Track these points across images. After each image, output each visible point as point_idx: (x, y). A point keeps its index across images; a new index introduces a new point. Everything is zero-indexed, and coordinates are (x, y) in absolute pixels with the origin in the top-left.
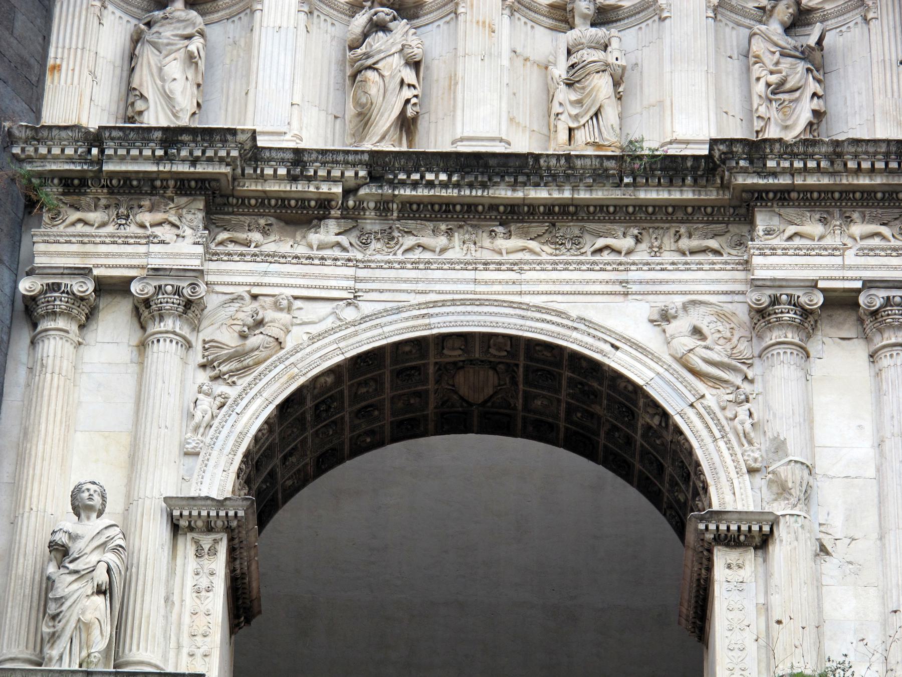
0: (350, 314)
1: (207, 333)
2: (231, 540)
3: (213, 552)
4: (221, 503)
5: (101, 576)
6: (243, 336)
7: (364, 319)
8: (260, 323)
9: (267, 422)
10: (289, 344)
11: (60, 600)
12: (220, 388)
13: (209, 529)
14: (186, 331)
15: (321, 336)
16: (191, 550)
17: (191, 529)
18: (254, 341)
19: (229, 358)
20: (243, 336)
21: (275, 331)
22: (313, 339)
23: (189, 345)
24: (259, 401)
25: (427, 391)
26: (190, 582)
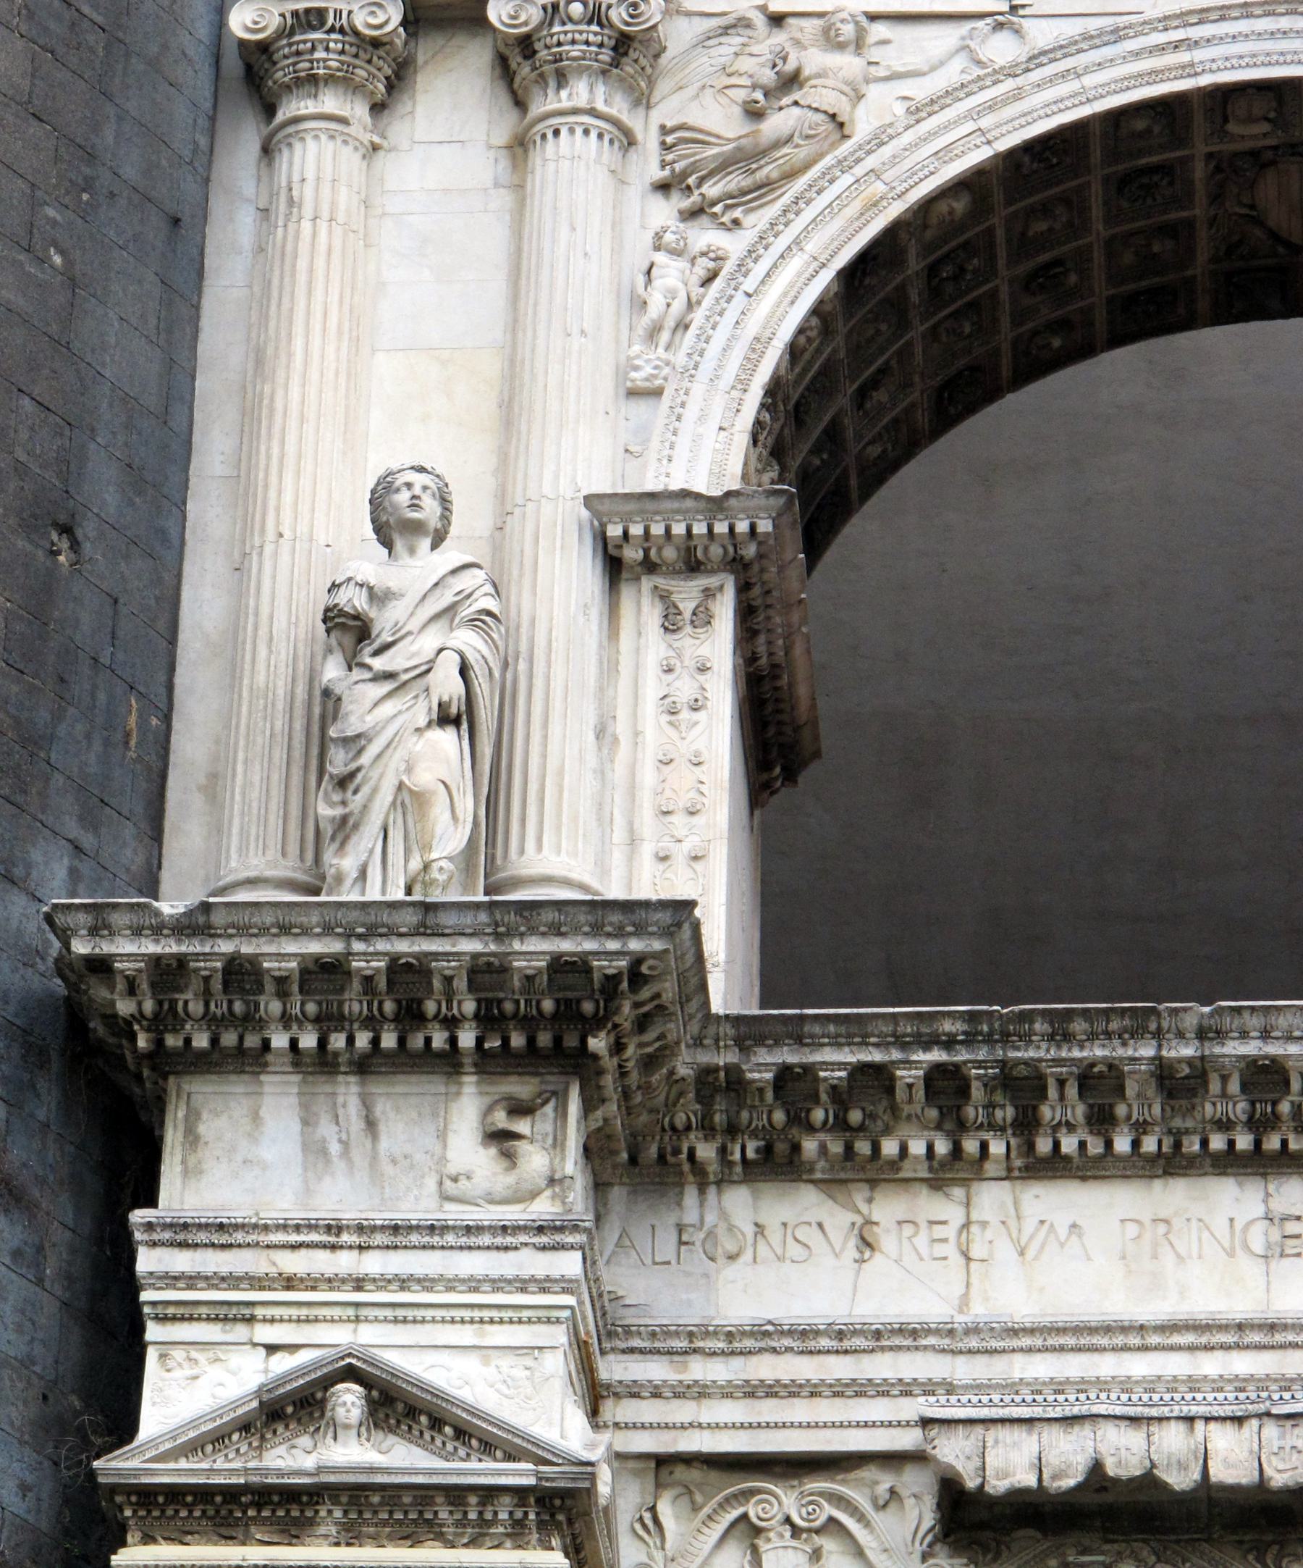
0: (1002, 49)
1: (668, 110)
2: (743, 588)
3: (702, 618)
4: (717, 505)
5: (447, 685)
6: (754, 113)
7: (1036, 59)
8: (791, 81)
9: (817, 310)
10: (863, 123)
11: (355, 743)
12: (705, 236)
13: (692, 565)
14: (619, 107)
15: (935, 104)
16: (652, 615)
17: (650, 566)
18: (779, 122)
19: (724, 166)
20: (754, 113)
21: (827, 98)
22: (918, 112)
23: (628, 140)
24: (796, 264)
25: (1190, 224)
26: (652, 688)
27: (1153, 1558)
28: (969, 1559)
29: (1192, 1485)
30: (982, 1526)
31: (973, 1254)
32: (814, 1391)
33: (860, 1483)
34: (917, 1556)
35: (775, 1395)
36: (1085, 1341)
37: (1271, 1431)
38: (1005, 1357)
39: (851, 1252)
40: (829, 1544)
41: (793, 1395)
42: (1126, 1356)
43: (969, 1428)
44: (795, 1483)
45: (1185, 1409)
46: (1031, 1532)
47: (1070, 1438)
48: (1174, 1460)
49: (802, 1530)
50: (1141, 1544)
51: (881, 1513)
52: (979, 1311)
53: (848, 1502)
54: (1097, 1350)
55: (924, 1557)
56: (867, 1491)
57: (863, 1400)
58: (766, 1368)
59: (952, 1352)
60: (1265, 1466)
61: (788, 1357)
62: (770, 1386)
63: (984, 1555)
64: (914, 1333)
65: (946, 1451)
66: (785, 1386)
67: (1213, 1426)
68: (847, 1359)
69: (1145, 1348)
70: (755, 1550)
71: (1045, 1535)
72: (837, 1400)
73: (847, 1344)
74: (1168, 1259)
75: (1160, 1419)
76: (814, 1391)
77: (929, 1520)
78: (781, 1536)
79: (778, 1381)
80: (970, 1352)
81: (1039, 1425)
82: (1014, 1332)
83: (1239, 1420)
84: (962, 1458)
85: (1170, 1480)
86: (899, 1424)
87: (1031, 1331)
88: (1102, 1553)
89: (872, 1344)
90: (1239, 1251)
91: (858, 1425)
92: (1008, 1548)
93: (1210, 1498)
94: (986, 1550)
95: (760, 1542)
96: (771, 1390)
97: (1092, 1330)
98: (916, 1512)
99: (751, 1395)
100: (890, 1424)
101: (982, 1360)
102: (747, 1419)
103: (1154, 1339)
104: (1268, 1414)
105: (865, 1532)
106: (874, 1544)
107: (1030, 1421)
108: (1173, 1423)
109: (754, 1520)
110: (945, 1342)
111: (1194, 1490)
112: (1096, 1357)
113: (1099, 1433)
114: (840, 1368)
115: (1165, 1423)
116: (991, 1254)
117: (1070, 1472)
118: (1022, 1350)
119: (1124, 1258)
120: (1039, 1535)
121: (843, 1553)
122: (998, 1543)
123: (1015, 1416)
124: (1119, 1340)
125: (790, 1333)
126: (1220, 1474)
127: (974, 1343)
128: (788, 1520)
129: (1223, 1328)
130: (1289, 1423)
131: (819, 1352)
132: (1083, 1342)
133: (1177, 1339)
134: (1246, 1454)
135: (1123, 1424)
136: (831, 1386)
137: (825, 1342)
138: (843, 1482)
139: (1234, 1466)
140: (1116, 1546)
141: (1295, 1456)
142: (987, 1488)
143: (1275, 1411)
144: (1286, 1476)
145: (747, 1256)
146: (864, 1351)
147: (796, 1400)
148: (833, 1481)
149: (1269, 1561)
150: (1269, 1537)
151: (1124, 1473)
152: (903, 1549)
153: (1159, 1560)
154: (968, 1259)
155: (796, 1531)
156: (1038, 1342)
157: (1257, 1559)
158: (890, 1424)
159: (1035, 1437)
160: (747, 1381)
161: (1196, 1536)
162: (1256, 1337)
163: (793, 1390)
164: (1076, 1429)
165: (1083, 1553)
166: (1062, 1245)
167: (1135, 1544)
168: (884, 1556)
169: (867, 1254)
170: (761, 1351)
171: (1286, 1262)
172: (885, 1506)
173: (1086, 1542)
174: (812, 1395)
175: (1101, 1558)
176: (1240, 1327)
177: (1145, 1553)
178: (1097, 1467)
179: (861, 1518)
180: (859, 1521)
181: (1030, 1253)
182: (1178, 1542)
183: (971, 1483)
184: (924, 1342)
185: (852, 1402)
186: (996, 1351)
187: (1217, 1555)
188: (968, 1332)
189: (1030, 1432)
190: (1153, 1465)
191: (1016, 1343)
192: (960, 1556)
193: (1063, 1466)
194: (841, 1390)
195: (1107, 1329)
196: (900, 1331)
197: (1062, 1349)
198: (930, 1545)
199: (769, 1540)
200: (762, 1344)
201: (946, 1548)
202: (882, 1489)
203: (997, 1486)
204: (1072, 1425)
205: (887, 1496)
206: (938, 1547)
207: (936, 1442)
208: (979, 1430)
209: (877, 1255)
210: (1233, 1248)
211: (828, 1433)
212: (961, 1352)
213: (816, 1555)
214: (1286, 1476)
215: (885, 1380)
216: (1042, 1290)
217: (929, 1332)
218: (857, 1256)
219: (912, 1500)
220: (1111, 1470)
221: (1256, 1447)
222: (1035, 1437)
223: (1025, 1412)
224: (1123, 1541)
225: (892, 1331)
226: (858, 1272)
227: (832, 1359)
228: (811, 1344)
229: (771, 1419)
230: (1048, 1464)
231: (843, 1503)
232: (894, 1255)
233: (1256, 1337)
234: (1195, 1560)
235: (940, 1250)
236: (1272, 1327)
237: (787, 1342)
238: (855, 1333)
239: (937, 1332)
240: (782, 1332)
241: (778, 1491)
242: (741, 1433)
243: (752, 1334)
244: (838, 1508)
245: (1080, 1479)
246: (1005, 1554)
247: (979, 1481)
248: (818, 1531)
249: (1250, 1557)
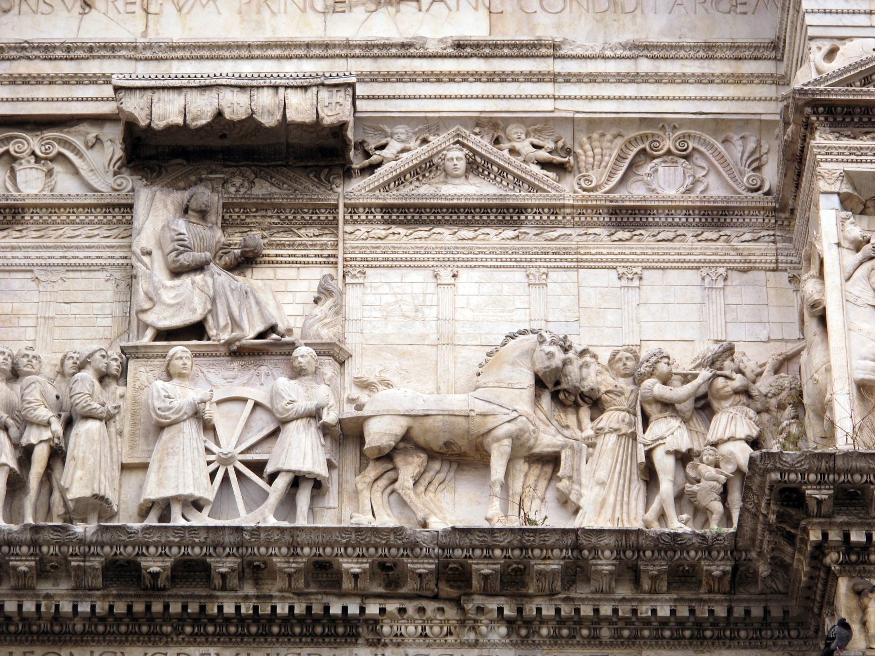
27: (253, 176)
28: (143, 176)
29: (276, 123)
30: (151, 158)
31: (149, 11)
32: (52, 80)
33: (79, 134)
34: (111, 173)
35: (28, 83)
36: (215, 53)
37: (324, 94)
38: (168, 63)
39: (78, 9)
40: (58, 168)
41: (38, 83)
42: (240, 62)
43: (143, 92)
44: (39, 133)
45: (273, 81)
46: (180, 161)
47: (203, 97)
48: (266, 110)
49: (42, 159)
50: (245, 168)
51: (90, 151)
52: (152, 37)
53: (70, 144)
54: (222, 58)
55: (115, 174)
56: (82, 138)
57: (81, 86)
58: (23, 68)
59: (136, 59)
60: (320, 112)
61: (37, 61)
62: (25, 78)
63: (152, 174)
64: (113, 48)
65: (129, 105)
66: (34, 78)
67: (289, 91)
68: (72, 63)
69: (252, 58)
70: (13, 171)
71: (188, 161)
72: (65, 86)
73: (72, 54)
74: (267, 14)
75: (258, 87)
76: (52, 80)
77: (119, 153)
78: (29, 162)
79: (30, 75)
80: (146, 59)
81: (184, 90)
82: (173, 48)
83: (305, 88)
84: (138, 109)
85: (263, 121)
86: (102, 99)
87: (184, 48)
88: (223, 173)
89: (88, 54)
90: (309, 10)
91: (77, 100)
92: (166, 170)
93: (288, 144)
94: (152, 171)
95: (17, 166)
96: (26, 80)
97: (220, 47)
98: (111, 149)
99: (13, 83)
100: (97, 100)
101: (153, 64)
102: (10, 96)
103: (257, 53)
104: (323, 85)
105: (80, 160)
106: (85, 167)
107: (179, 88)
108: (265, 89)
109: (13, 153)
110: (132, 54)
111: (276, 126)
112: (221, 63)
113: (221, 95)
114: (68, 68)
115: (261, 90)
116: (161, 10)
117: (203, 116)
118: (177, 58)
119: (240, 13)
120: (185, 163)
121: (66, 173)
122: (160, 167)
123: (171, 85)
124: (236, 53)
125: (38, 48)
126: (292, 116)
127: (148, 54)
128: (33, 153)
129: (298, 46)
130: (335, 90)
131: (56, 59)
132: (214, 54)
133: (270, 52)
134: (309, 106)
135: (236, 90)
136: (62, 77)
137: (59, 53)
138: (68, 133)
139: (302, 113)
140: (231, 170)
141: (338, 107)
142: (152, 125)
143: (327, 82)
144: (332, 118)
145: (15, 10)
146: (82, 58)
147: (40, 86)
148: (61, 132)
149: (322, 178)
150: (322, 163)
151: (235, 118)
152: (103, 170)
153: (256, 177)
154: (148, 13)
155: (38, 159)
156: (188, 54)
157: (315, 176)
158: (97, 100)
159: (182, 97)
160: (11, 75)
161: (278, 163)
162: (317, 52)
163: (39, 80)
164: (208, 93)
165: (211, 173)
166: (204, 6)
167: (242, 168)
168: (91, 174)
169: (87, 10)
170: (20, 58)
171: (336, 15)
172: (92, 147)
173: (214, 167)
174: (50, 83)
175: (222, 176)
176: (308, 46)
177: (248, 173)
178: (219, 114)
179: (78, 153)
180: (76, 155)
181: (185, 10)
182: (268, 167)
183: (143, 123)
184: (119, 54)
185: (74, 87)
186: (162, 59)
187: (291, 174)
188: (145, 48)
189: (179, 95)
190: (253, 112)
191: (173, 54)
192: (137, 175)
193: (199, 113)
194: (68, 80)
195: (229, 46)
196: (104, 47)
197: (201, 58)
198: (119, 168)
199: (21, 164)
200: (21, 54)
201: (129, 170)
202: (91, 137)
203: (159, 124)
204: (205, 91)
205: (94, 141)
206: (124, 170)
207: (123, 100)
208: (149, 93)
209: (93, 11)
210: (305, 8)
211: (60, 104)
212: (141, 59)
213: (50, 173)
214: (332, 118)
215: (94, 74)
216: (191, 29)
217: (122, 47)
218: (81, 11)
219: (109, 143)
220: (228, 115)
221: (315, 102)
222: (182, 97)
223: (177, 83)
224: (235, 166)
225: (100, 47)
226: (81, 19)
227: (63, 63)
228: (51, 55)
229: (25, 96)
230: (190, 112)
231: (67, 145)
232: (103, 10)
233: (317, 52)
234: (278, 177)
235: (130, 8)
236: (327, 46)
237: (36, 53)
238: (77, 48)
239: (127, 48)
240: (33, 48)
241: (28, 137)
242: (7, 104)
243: (15, 48)
244: (64, 147)
245: (209, 120)
246: (164, 173)
247: (148, 121)
248: (52, 160)
249: (311, 175)
